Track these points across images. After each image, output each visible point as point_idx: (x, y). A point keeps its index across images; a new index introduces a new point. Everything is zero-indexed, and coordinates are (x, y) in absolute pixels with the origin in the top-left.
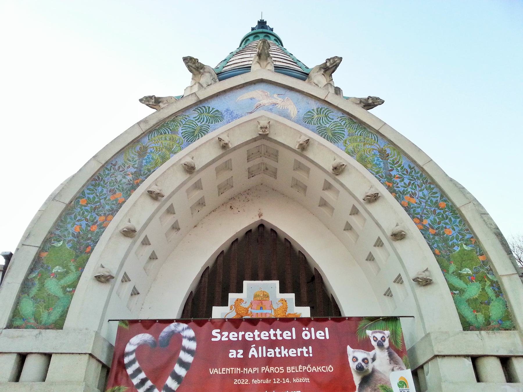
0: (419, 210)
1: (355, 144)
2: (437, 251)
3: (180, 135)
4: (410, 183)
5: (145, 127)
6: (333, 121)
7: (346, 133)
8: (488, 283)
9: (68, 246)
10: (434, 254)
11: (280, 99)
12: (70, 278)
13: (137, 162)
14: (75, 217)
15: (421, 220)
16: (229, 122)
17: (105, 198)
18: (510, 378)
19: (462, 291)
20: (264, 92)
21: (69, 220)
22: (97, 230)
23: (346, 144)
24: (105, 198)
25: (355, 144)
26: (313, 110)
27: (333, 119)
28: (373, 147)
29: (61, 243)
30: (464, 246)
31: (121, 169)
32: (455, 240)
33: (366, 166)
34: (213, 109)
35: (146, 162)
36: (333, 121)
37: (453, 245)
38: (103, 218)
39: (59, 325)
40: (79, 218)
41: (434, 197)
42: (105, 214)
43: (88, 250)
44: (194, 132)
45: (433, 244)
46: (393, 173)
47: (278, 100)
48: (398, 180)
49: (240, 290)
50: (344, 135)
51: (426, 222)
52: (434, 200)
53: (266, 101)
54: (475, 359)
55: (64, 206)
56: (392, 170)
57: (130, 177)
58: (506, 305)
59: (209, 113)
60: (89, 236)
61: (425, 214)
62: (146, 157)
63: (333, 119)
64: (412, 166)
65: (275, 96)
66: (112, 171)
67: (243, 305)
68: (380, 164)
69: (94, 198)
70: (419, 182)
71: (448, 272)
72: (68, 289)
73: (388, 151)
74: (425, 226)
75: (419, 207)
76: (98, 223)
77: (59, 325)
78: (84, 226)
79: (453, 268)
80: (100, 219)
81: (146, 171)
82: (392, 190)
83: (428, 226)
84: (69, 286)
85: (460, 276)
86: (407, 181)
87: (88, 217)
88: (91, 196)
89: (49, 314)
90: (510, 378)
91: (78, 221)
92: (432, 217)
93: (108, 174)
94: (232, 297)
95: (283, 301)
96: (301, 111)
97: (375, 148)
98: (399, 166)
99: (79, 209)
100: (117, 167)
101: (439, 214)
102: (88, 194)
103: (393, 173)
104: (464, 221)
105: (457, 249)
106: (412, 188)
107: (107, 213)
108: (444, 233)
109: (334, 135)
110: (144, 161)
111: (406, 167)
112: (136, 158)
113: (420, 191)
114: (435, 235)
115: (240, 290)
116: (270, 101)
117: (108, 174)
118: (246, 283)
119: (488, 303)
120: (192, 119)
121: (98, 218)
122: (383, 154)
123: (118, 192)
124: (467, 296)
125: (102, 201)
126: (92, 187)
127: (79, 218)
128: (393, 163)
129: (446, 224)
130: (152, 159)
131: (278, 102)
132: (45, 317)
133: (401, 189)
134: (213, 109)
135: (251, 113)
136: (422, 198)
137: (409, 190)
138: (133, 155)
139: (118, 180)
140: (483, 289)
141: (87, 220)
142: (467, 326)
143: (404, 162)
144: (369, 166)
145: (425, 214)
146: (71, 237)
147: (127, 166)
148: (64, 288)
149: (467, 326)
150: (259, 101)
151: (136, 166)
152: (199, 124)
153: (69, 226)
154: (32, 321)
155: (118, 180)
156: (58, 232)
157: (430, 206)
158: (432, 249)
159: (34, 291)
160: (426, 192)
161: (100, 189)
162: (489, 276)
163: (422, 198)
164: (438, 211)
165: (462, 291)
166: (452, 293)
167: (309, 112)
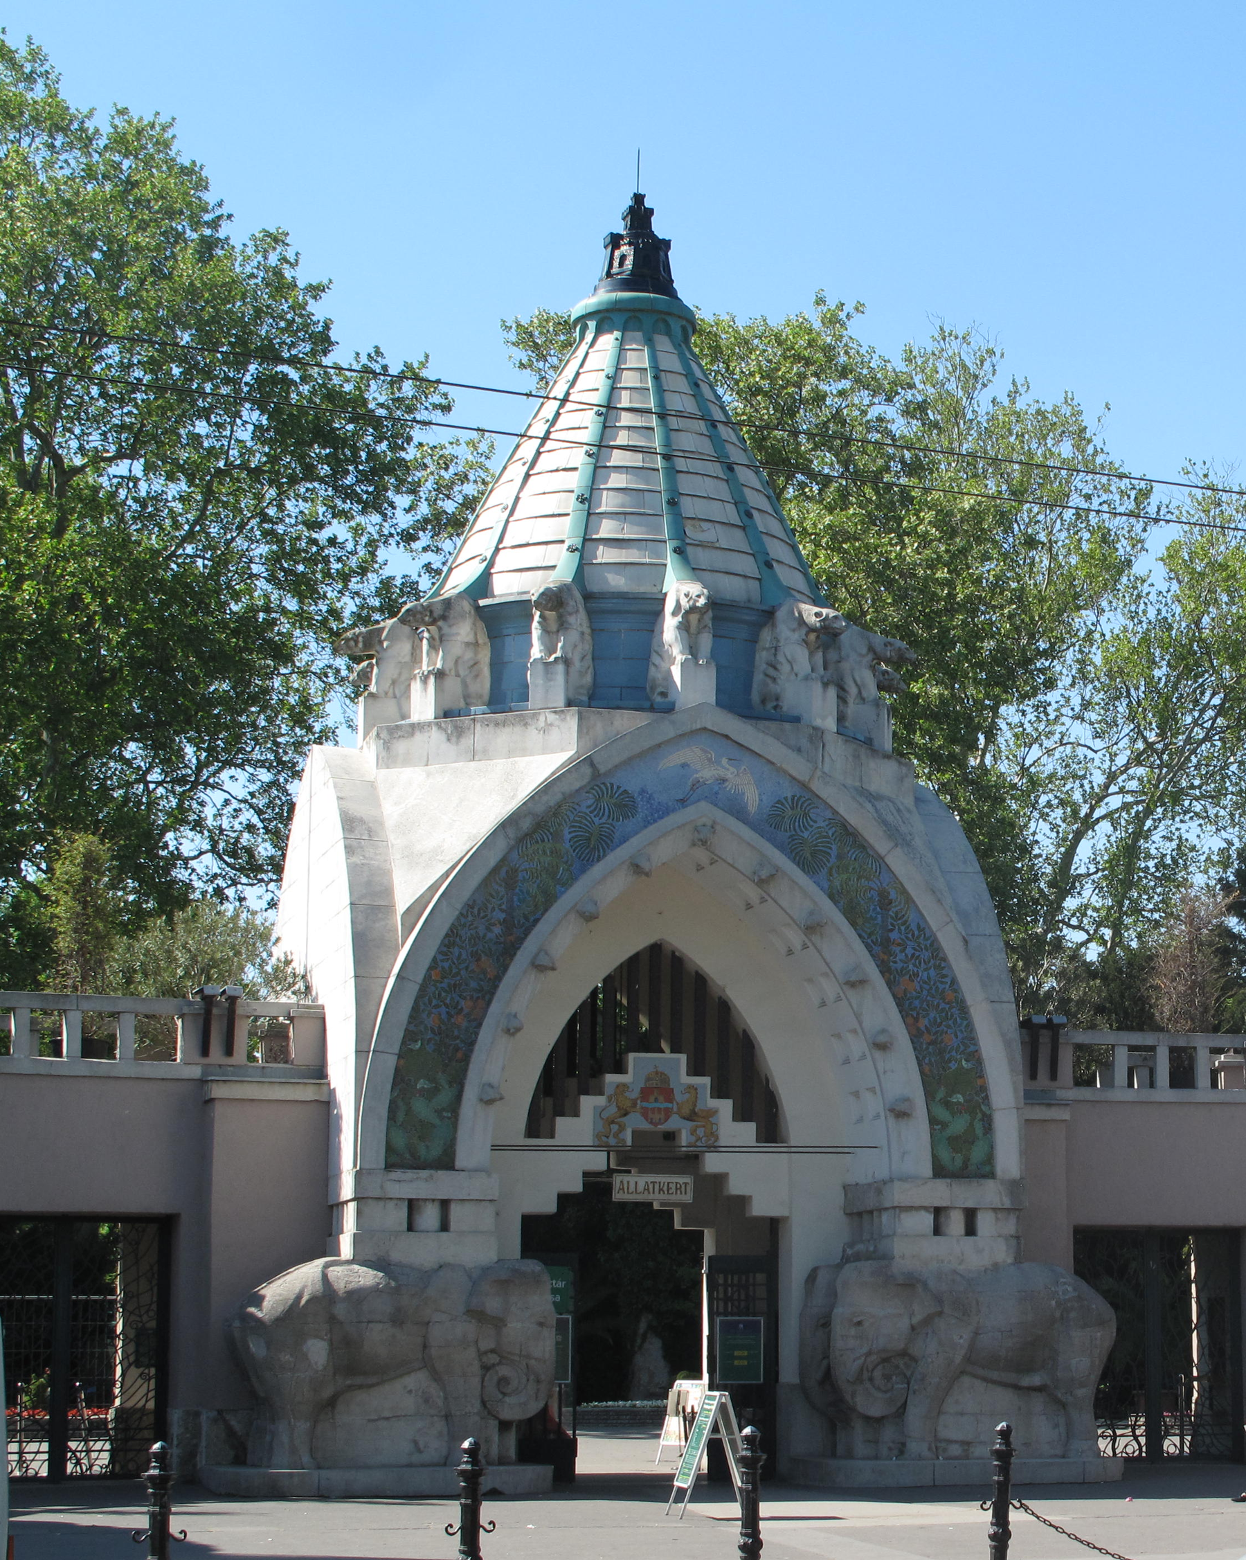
0: (917, 1002)
1: (845, 876)
2: (927, 1068)
3: (567, 845)
4: (913, 955)
5: (511, 833)
6: (816, 825)
7: (834, 853)
8: (979, 1116)
9: (430, 1048)
10: (922, 1073)
11: (732, 769)
12: (445, 1097)
13: (505, 900)
14: (430, 1002)
15: (916, 1019)
16: (647, 823)
17: (467, 968)
18: (970, 1230)
19: (944, 1125)
20: (705, 752)
21: (422, 1007)
22: (465, 1024)
23: (831, 875)
24: (467, 968)
25: (845, 876)
26: (786, 798)
27: (815, 822)
28: (872, 884)
29: (419, 1043)
30: (964, 1062)
31: (482, 914)
32: (954, 1053)
33: (853, 924)
34: (619, 787)
35: (519, 900)
36: (816, 825)
37: (950, 1061)
38: (470, 1003)
39: (446, 1162)
40: (434, 1002)
41: (942, 983)
42: (472, 997)
43: (459, 1055)
44: (589, 839)
45: (924, 1058)
46: (894, 936)
47: (729, 771)
48: (898, 949)
49: (620, 1068)
50: (829, 854)
51: (923, 1023)
52: (941, 987)
53: (707, 774)
54: (938, 1212)
55: (417, 987)
56: (892, 930)
57: (497, 930)
58: (992, 1147)
59: (612, 797)
60: (456, 1033)
61: (924, 1010)
62: (517, 890)
63: (815, 822)
64: (922, 925)
65: (724, 761)
66: (470, 918)
67: (627, 1094)
68: (876, 918)
69: (450, 967)
70: (925, 955)
71: (933, 1098)
72: (445, 1114)
73: (893, 895)
74: (918, 1029)
75: (917, 998)
76: (466, 1011)
77: (446, 1162)
78: (444, 1016)
79: (941, 1094)
80: (466, 1005)
81: (522, 920)
82: (884, 969)
83: (923, 1029)
84: (444, 1109)
85: (947, 1104)
86: (909, 951)
87: (448, 1001)
88: (446, 965)
89: (427, 1147)
90: (970, 1230)
91: (436, 1006)
92: (932, 1014)
93: (464, 926)
94: (611, 1079)
95: (692, 1089)
96: (764, 798)
97: (873, 886)
98: (904, 924)
99: (433, 989)
100: (476, 911)
101: (943, 1009)
102: (442, 961)
103: (894, 936)
104: (970, 1027)
105: (953, 1066)
106: (915, 965)
107: (475, 995)
108: (942, 1042)
109: (813, 854)
110: (515, 898)
111: (914, 926)
112: (502, 891)
113: (925, 970)
114: (929, 1044)
115: (620, 1068)
116: (715, 772)
117: (464, 926)
118: (632, 1057)
119: (973, 1143)
120: (584, 810)
121: (462, 1002)
122: (885, 902)
123: (484, 958)
124: (949, 1132)
125: (463, 972)
126: (445, 949)
127: (434, 1002)
128: (897, 918)
129: (949, 1027)
130: (528, 893)
131: (729, 776)
132: (422, 1150)
133: (899, 965)
134: (619, 787)
135: (683, 802)
136: (925, 982)
137: (911, 967)
138: (497, 887)
139: (481, 934)
140: (971, 1124)
141: (446, 1005)
142: (940, 1171)
143: (911, 916)
144: (860, 921)
145: (924, 1010)
146: (429, 1035)
147: (490, 907)
148: (439, 1112)
149: (940, 1171)
150: (697, 772)
151: (504, 907)
152: (596, 820)
153: (424, 1016)
154: (408, 1156)
155: (481, 934)
156: (412, 1028)
157: (933, 997)
158: (920, 1065)
159: (401, 1116)
160: (932, 972)
161: (456, 951)
162: (983, 1107)
163: (925, 982)
164: (942, 1005)
165: (944, 1125)
166: (932, 1129)
167: (779, 802)
